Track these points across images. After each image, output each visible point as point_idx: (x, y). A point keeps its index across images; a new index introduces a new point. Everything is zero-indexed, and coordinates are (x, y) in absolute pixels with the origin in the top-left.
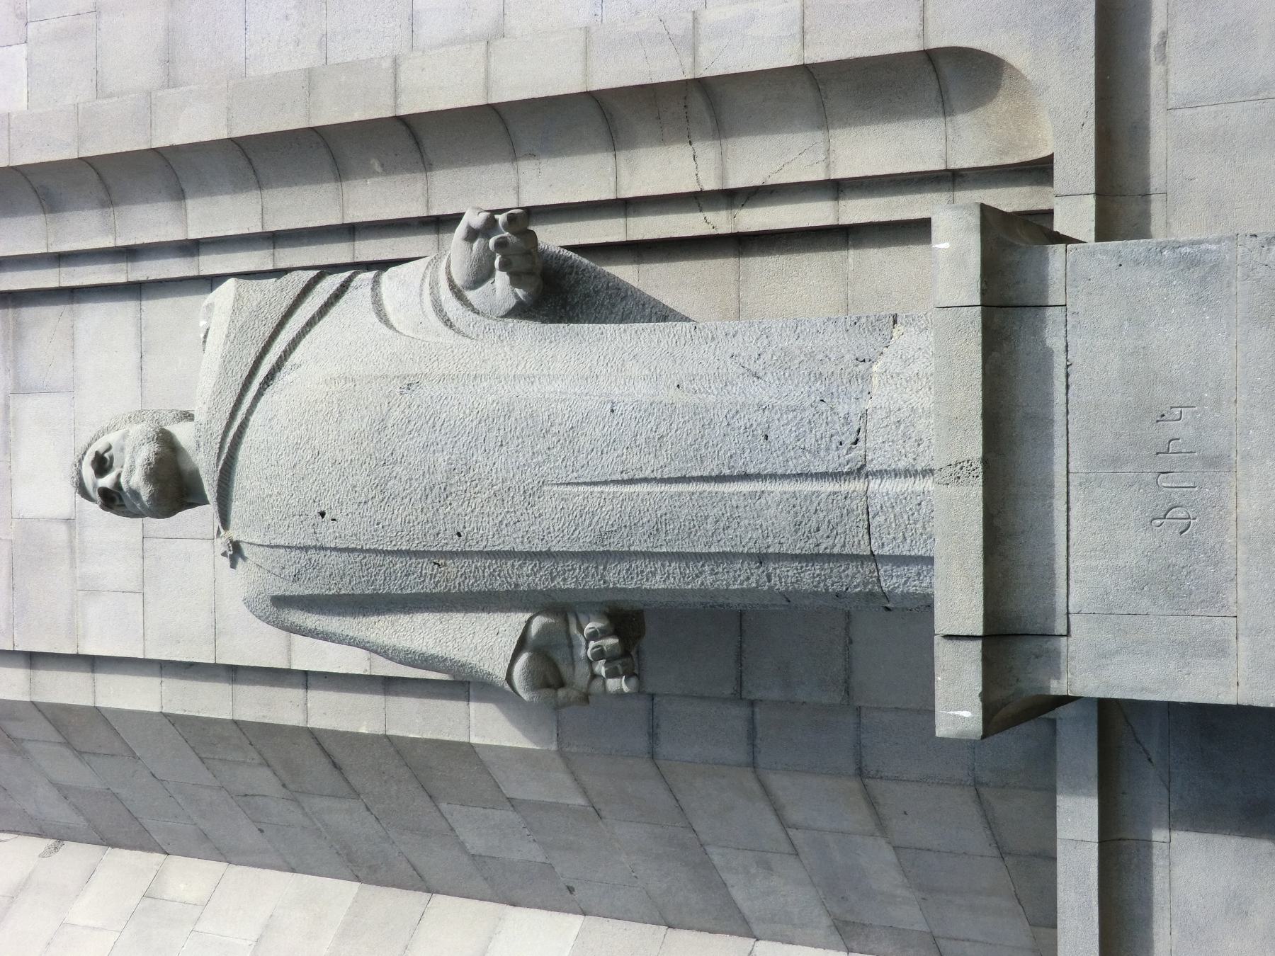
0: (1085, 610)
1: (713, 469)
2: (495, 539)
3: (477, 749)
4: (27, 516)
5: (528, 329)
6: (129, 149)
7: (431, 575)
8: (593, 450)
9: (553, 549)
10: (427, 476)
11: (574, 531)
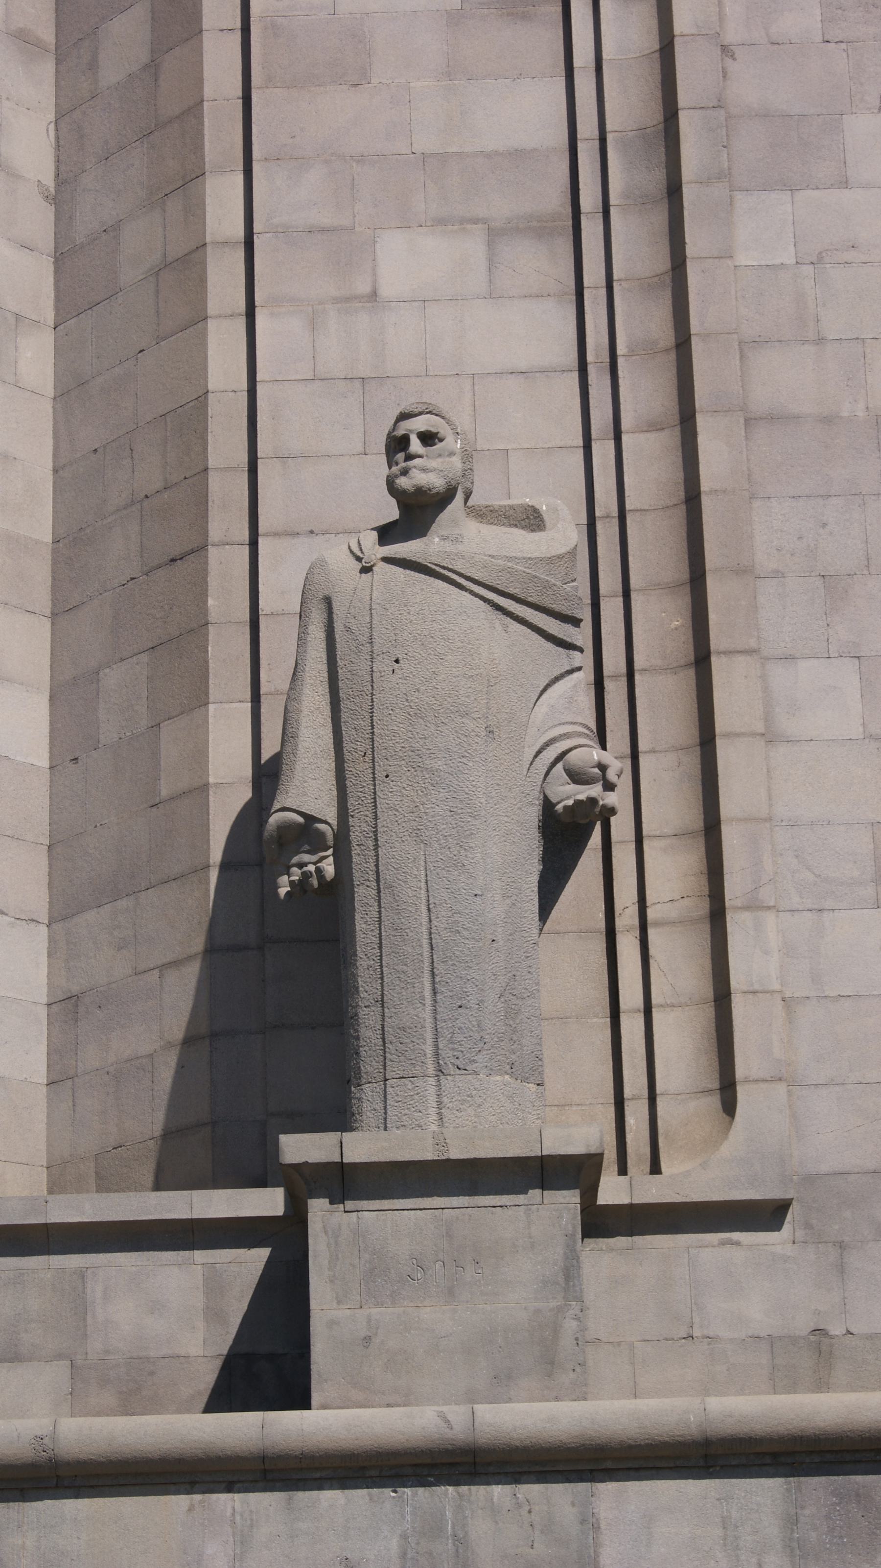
3: (203, 708)
4: (378, 246)
5: (533, 814)
6: (696, 388)
8: (449, 881)
9: (379, 849)
10: (428, 752)
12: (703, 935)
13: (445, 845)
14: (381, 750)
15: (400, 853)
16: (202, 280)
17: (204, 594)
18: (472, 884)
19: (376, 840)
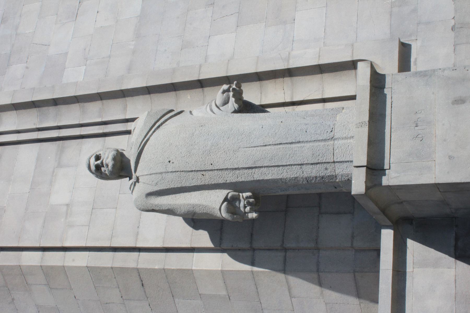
0: (394, 162)
1: (290, 141)
2: (222, 165)
3: (194, 272)
7: (200, 179)
8: (255, 138)
9: (239, 167)
10: (204, 148)
11: (247, 161)
12: (297, 79)
13: (241, 140)
14: (201, 167)
15: (242, 158)
16: (52, 267)
17: (154, 270)
18: (258, 129)
19: (236, 169)
